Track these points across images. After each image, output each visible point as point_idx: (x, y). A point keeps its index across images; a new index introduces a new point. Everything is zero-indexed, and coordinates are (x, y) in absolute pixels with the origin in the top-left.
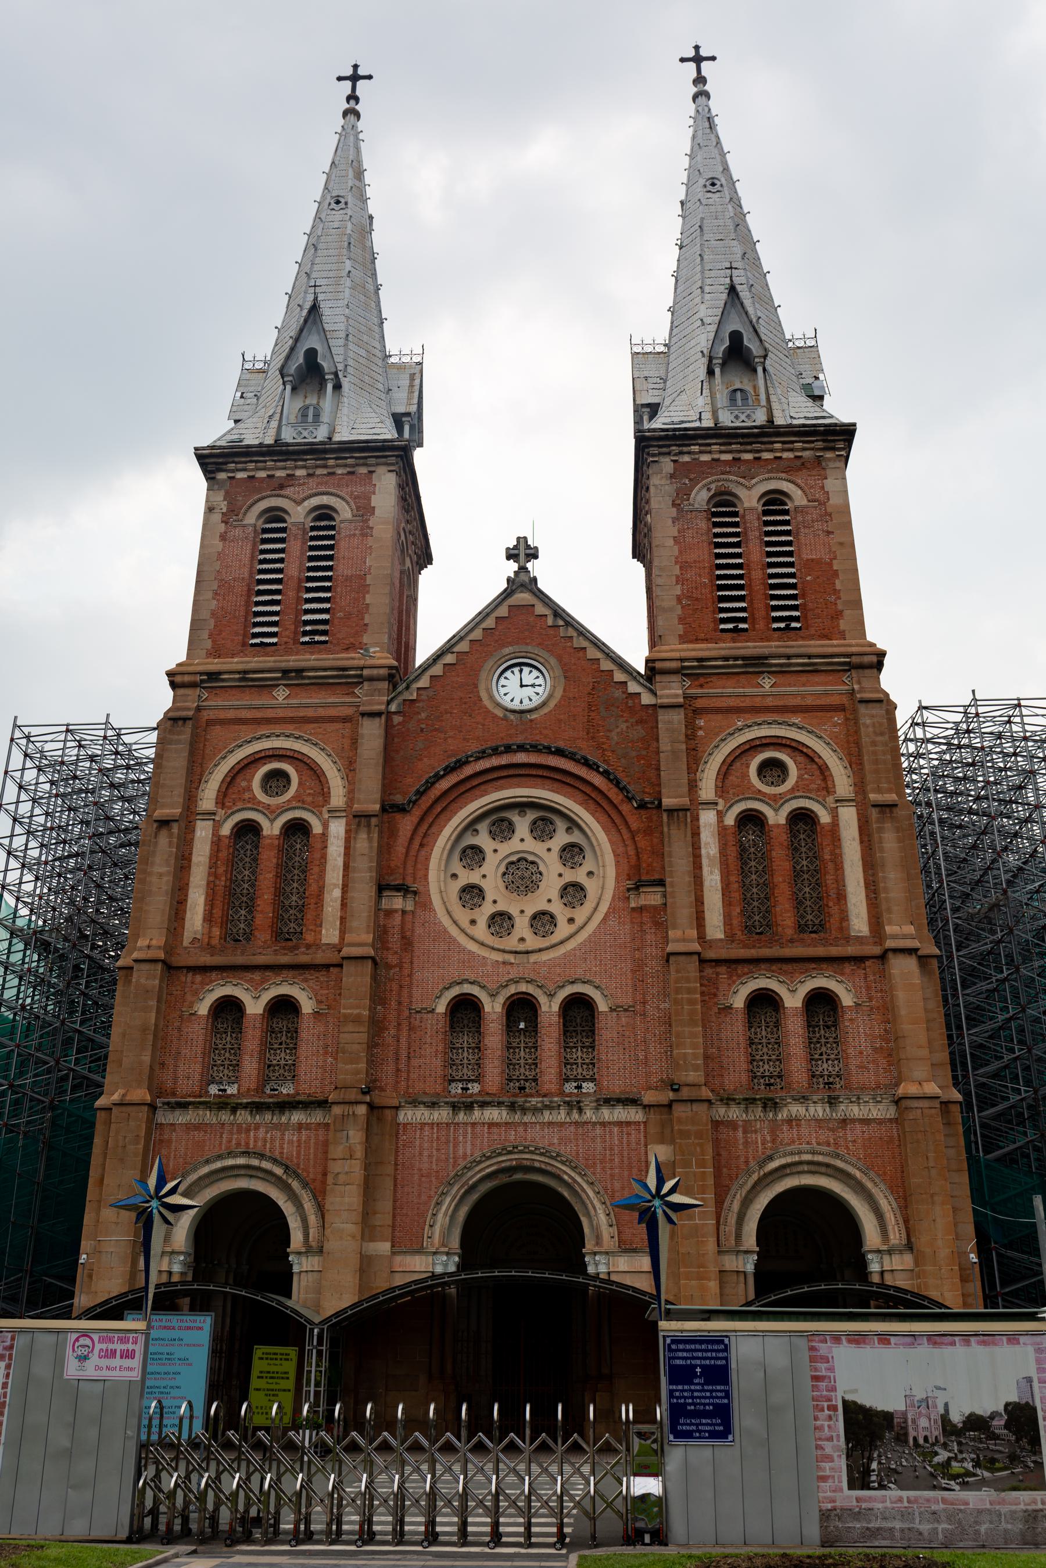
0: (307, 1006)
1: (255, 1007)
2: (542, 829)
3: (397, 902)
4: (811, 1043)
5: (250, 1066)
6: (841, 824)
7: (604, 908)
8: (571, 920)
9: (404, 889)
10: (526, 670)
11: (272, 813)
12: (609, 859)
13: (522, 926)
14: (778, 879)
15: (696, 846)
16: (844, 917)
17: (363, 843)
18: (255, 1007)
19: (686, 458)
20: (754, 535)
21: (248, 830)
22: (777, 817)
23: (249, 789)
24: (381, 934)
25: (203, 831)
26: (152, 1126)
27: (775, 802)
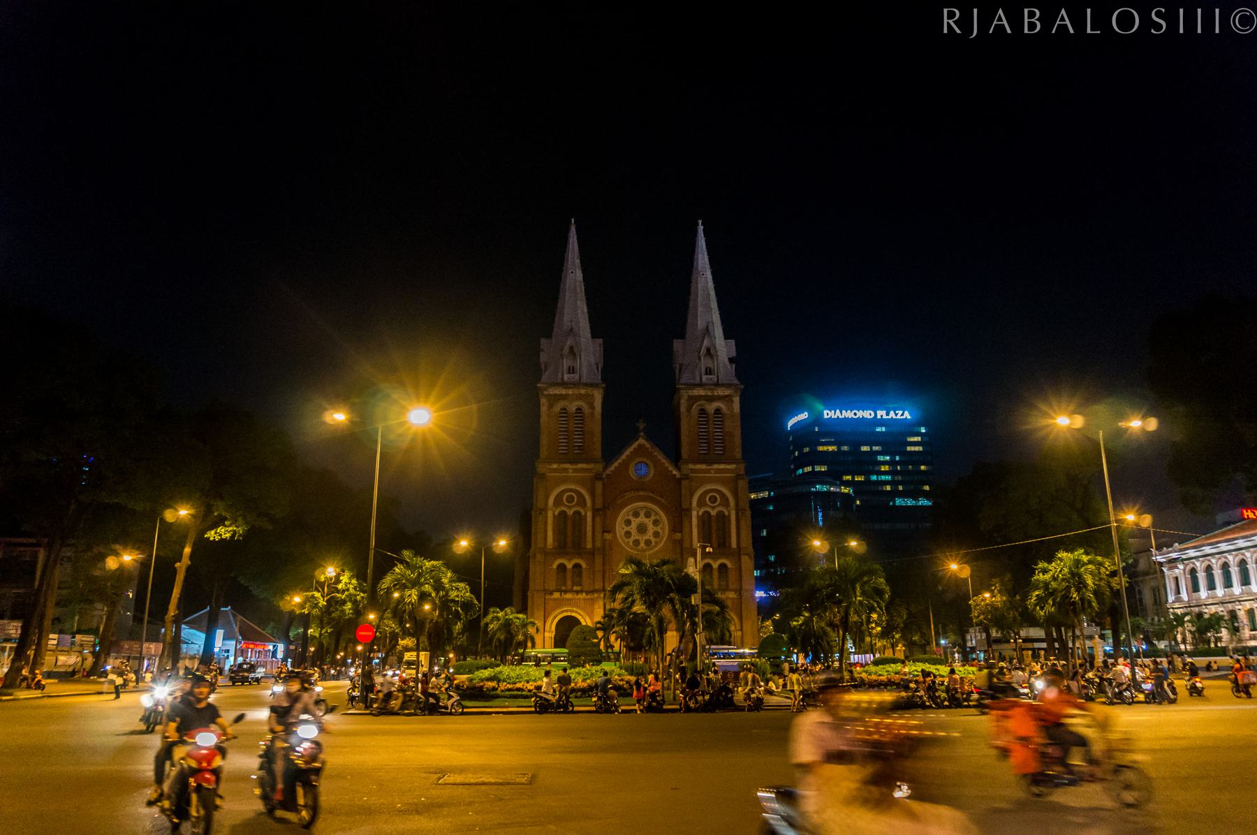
0: (584, 566)
1: (569, 566)
2: (648, 515)
3: (608, 536)
4: (720, 577)
5: (569, 583)
6: (731, 515)
7: (665, 539)
8: (656, 542)
9: (608, 532)
10: (643, 464)
11: (570, 508)
12: (666, 523)
13: (642, 544)
14: (713, 531)
15: (691, 522)
16: (730, 543)
17: (598, 519)
18: (569, 566)
19: (691, 394)
20: (711, 422)
21: (563, 514)
22: (713, 513)
23: (562, 500)
24: (604, 544)
25: (550, 514)
26: (545, 599)
27: (713, 508)
